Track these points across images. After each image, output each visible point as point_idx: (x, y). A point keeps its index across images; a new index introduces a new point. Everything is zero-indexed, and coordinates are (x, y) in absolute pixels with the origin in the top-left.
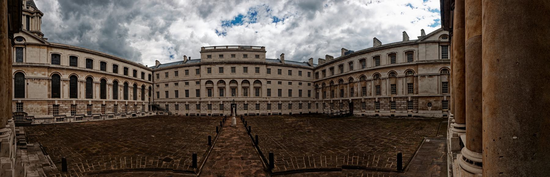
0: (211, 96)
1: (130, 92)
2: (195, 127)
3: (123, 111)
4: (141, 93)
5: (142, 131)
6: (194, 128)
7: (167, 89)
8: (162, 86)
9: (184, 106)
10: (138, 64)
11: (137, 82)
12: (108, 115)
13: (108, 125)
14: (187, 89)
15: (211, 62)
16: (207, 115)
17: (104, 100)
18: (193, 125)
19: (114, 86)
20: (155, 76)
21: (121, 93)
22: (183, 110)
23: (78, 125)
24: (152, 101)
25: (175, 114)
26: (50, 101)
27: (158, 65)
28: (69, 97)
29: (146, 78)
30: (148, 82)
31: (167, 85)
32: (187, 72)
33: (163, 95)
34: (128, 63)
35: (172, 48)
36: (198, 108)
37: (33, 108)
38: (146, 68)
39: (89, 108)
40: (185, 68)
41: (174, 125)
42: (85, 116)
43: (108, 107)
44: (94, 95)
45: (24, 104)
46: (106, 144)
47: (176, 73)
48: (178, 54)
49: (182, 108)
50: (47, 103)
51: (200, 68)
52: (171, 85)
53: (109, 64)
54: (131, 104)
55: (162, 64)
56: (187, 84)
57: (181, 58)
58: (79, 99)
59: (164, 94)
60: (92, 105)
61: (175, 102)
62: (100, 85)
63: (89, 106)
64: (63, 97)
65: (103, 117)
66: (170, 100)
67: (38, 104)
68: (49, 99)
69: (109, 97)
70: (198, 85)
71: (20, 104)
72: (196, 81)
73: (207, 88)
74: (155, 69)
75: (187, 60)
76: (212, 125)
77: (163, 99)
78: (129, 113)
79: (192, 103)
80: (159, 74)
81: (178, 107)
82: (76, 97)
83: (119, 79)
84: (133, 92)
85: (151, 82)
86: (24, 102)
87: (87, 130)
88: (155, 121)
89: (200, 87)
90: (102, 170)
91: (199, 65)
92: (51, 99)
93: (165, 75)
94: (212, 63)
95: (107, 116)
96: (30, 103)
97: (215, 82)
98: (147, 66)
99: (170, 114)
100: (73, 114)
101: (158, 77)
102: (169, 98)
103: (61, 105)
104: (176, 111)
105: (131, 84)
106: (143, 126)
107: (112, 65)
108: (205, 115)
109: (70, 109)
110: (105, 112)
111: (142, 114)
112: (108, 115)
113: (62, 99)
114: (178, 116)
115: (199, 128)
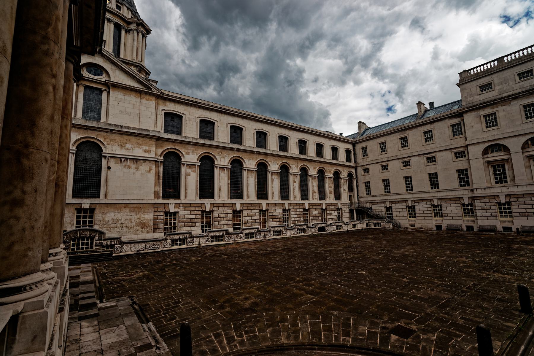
0: (506, 182)
1: (313, 186)
2: (467, 257)
3: (300, 222)
4: (333, 186)
5: (338, 260)
6: (464, 259)
8: (375, 170)
9: (429, 209)
10: (325, 133)
11: (323, 165)
12: (273, 229)
13: (273, 249)
14: (433, 172)
15: (494, 98)
16: (500, 227)
17: (264, 202)
18: (460, 251)
19: (281, 175)
20: (359, 152)
21: (295, 187)
22: (428, 218)
23: (215, 251)
24: (356, 200)
25: (409, 226)
26: (159, 206)
27: (363, 130)
28: (198, 197)
29: (342, 157)
30: (345, 164)
32: (429, 136)
33: (377, 188)
34: (306, 132)
35: (390, 92)
36: (469, 213)
38: (340, 139)
39: (237, 217)
40: (423, 127)
41: (409, 250)
42: (229, 234)
43: (271, 214)
44: (245, 193)
45: (97, 211)
46: (270, 288)
47: (404, 142)
48: (404, 101)
49: (425, 212)
50: (152, 210)
51: (463, 120)
52: (395, 166)
53: (271, 136)
54: (314, 207)
55: (371, 127)
56: (432, 160)
57: (412, 108)
58: (217, 200)
59: (381, 185)
61: (406, 201)
62: (255, 173)
64: (186, 197)
65: (262, 234)
69: (273, 197)
70: (461, 159)
71: (85, 210)
72: (453, 151)
73: (488, 163)
74: (358, 138)
75: (426, 111)
76: (521, 255)
77: (380, 196)
78: (313, 225)
79: (449, 202)
80: (366, 148)
81: (415, 211)
82: (212, 196)
83: (291, 163)
84: (317, 185)
85: (352, 164)
86: (98, 206)
87: (234, 259)
88: (364, 240)
89: (467, 164)
90: (264, 344)
91: (460, 115)
92: (160, 201)
93: (379, 149)
94: (496, 100)
95: (270, 231)
96: (112, 210)
97: (515, 145)
98: (341, 134)
99: (397, 226)
100: (206, 230)
102: (391, 193)
103: (181, 213)
104: (412, 221)
105: (313, 171)
106: (340, 250)
107: (276, 137)
108: (492, 230)
110: (267, 225)
111: (337, 226)
112: (273, 229)
113: (183, 200)
114: (416, 230)
115: (480, 262)
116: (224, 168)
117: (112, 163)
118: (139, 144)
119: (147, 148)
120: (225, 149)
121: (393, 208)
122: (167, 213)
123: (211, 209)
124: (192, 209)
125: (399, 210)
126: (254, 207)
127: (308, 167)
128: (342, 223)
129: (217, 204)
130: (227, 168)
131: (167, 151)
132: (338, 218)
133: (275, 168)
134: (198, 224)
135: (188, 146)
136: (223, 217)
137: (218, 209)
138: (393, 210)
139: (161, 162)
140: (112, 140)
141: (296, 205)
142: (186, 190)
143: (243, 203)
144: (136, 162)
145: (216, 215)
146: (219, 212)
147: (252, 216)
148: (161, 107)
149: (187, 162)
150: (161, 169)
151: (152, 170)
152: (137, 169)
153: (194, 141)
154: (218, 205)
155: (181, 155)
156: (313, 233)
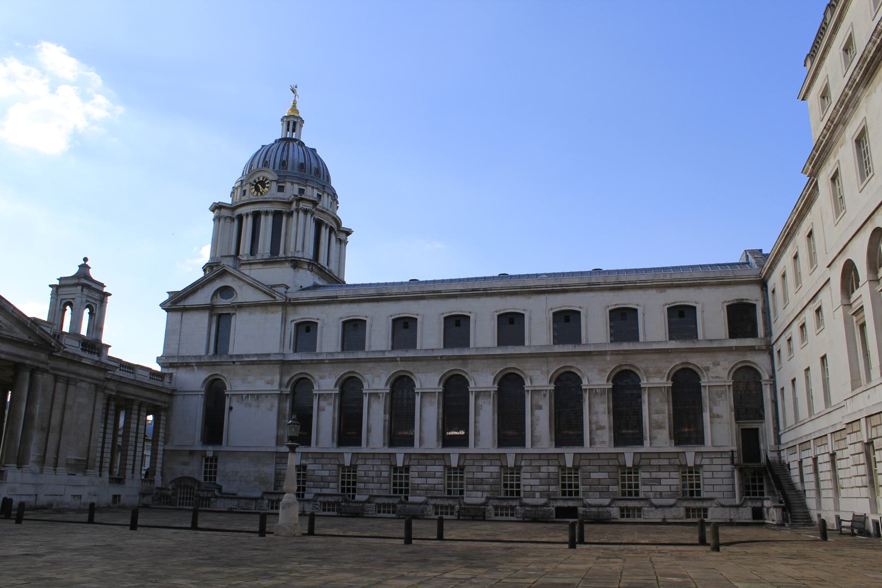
45: (219, 460)
64: (317, 443)
71: (212, 459)
109: (334, 479)
113: (313, 449)
119: (270, 378)
120: (381, 361)
123: (354, 463)
124: (324, 461)
126: (433, 461)
130: (383, 393)
131: (296, 378)
134: (332, 485)
136: (373, 477)
141: (537, 457)
143: (410, 454)
144: (258, 397)
146: (366, 468)
147: (427, 478)
148: (291, 317)
150: (287, 405)
151: (274, 407)
152: (258, 406)
153: (330, 357)
154: (365, 456)
155: (313, 381)
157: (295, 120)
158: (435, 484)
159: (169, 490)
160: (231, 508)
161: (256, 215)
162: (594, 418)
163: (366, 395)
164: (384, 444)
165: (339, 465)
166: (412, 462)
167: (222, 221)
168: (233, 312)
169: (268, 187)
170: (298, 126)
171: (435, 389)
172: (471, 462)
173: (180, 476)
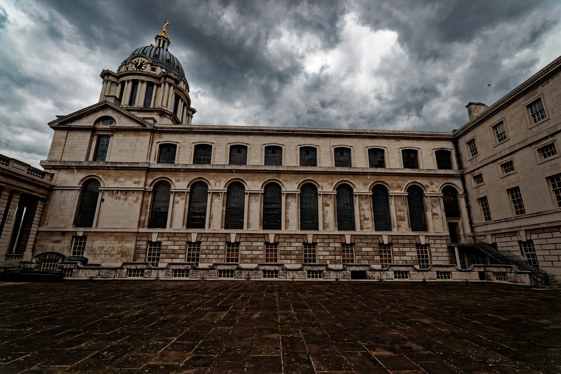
7: (512, 181)
26: (143, 235)
31: (508, 167)
37: (103, 248)
45: (88, 239)
60: (237, 244)
63: (233, 247)
64: (171, 226)
65: (244, 274)
66: (534, 221)
67: (115, 239)
68: (141, 230)
71: (81, 238)
86: (89, 234)
96: (99, 238)
101: (474, 152)
113: (168, 230)
116: (219, 193)
117: (106, 197)
118: (130, 177)
119: (137, 180)
121: (535, 242)
122: (150, 243)
123: (198, 240)
124: (176, 239)
125: (547, 247)
127: (352, 183)
128: (411, 268)
129: (206, 234)
130: (222, 193)
132: (419, 261)
133: (293, 188)
134: (181, 256)
135: (179, 173)
136: (213, 250)
137: (206, 240)
138: (536, 247)
139: (150, 192)
140: (109, 176)
141: (327, 237)
142: (172, 218)
143: (241, 234)
144: (126, 193)
145: (203, 247)
146: (208, 243)
147: (252, 251)
148: (156, 140)
149: (175, 189)
152: (126, 199)
153: (184, 167)
154: (207, 235)
155: (171, 183)
156: (339, 280)
157: (165, 40)
158: (258, 255)
159: (33, 263)
160: (92, 277)
161: (135, 83)
162: (362, 213)
163: (210, 194)
164: (222, 227)
165: (188, 242)
166: (242, 239)
167: (109, 83)
168: (111, 134)
169: (144, 66)
170: (166, 44)
171: (259, 191)
172: (283, 240)
173: (49, 251)
